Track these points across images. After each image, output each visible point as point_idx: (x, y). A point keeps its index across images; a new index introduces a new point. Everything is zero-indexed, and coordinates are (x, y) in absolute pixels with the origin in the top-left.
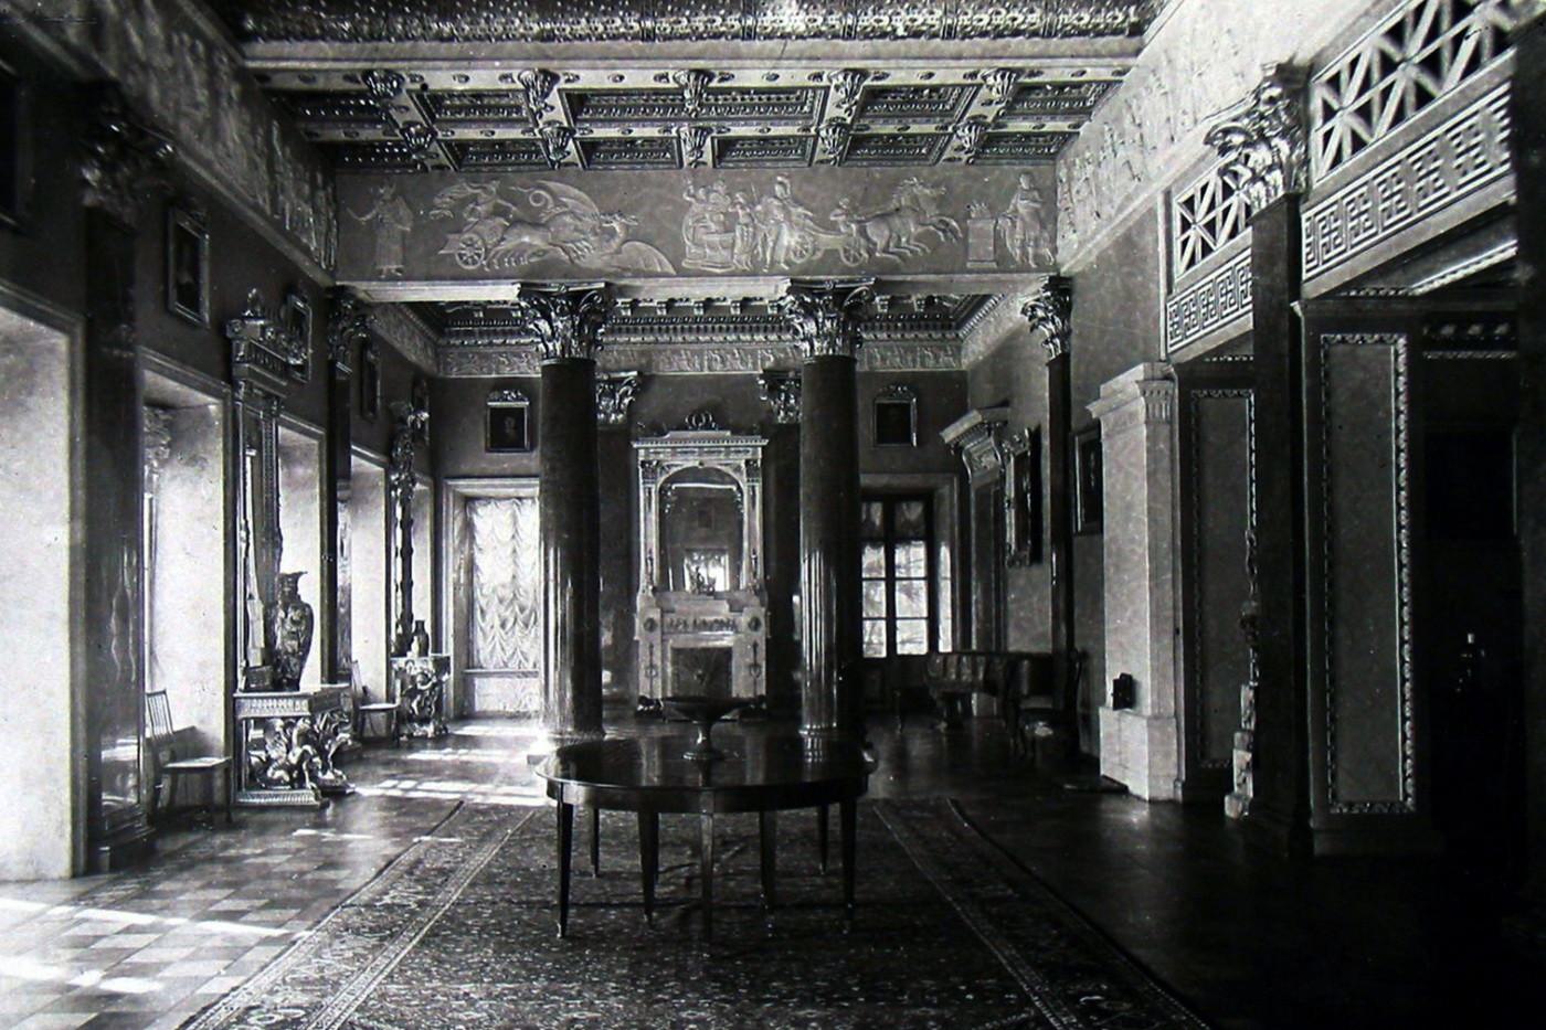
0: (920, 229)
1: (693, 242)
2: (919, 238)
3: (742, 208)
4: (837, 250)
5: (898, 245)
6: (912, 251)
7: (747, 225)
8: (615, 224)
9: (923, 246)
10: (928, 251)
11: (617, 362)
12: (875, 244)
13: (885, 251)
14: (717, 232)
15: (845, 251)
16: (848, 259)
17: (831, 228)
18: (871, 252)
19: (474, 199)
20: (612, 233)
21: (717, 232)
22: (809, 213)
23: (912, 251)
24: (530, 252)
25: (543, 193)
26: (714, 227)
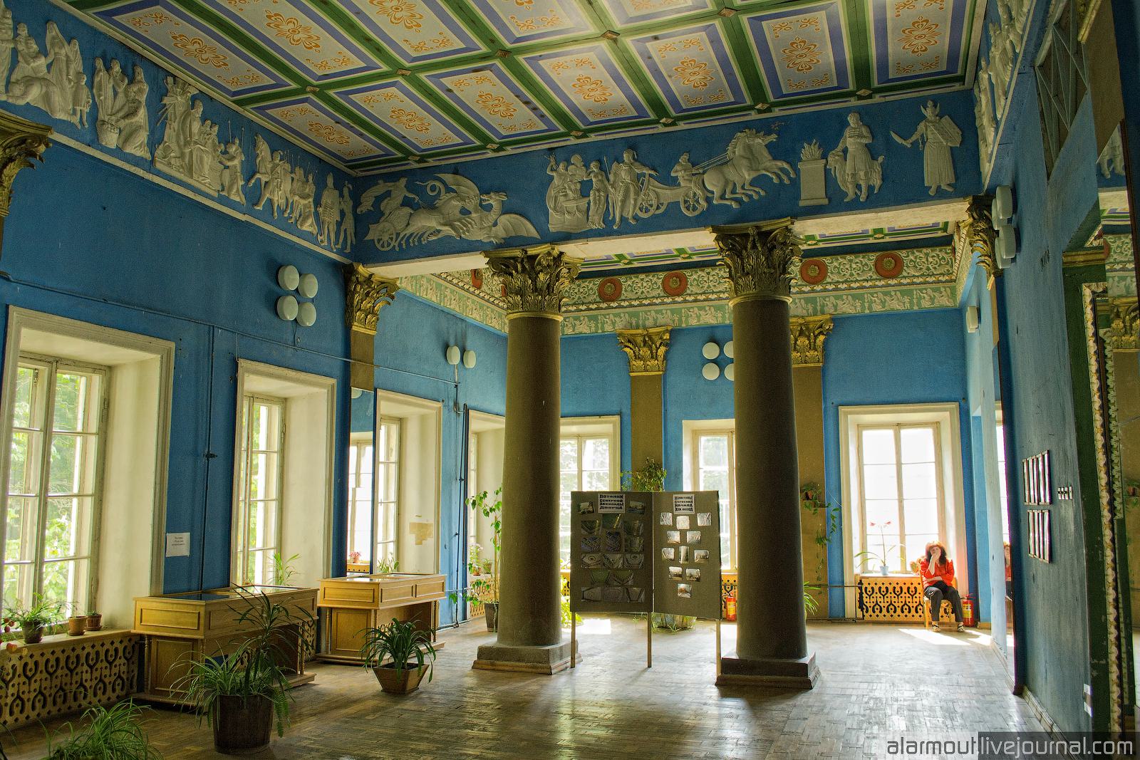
0: (754, 175)
1: (555, 209)
2: (753, 183)
5: (733, 192)
6: (747, 195)
7: (598, 191)
8: (491, 202)
9: (757, 189)
10: (762, 193)
11: (655, 320)
12: (713, 193)
13: (722, 197)
15: (686, 202)
16: (688, 208)
17: (674, 183)
18: (708, 200)
19: (388, 194)
20: (489, 208)
22: (652, 172)
23: (747, 195)
24: (428, 233)
25: (438, 184)
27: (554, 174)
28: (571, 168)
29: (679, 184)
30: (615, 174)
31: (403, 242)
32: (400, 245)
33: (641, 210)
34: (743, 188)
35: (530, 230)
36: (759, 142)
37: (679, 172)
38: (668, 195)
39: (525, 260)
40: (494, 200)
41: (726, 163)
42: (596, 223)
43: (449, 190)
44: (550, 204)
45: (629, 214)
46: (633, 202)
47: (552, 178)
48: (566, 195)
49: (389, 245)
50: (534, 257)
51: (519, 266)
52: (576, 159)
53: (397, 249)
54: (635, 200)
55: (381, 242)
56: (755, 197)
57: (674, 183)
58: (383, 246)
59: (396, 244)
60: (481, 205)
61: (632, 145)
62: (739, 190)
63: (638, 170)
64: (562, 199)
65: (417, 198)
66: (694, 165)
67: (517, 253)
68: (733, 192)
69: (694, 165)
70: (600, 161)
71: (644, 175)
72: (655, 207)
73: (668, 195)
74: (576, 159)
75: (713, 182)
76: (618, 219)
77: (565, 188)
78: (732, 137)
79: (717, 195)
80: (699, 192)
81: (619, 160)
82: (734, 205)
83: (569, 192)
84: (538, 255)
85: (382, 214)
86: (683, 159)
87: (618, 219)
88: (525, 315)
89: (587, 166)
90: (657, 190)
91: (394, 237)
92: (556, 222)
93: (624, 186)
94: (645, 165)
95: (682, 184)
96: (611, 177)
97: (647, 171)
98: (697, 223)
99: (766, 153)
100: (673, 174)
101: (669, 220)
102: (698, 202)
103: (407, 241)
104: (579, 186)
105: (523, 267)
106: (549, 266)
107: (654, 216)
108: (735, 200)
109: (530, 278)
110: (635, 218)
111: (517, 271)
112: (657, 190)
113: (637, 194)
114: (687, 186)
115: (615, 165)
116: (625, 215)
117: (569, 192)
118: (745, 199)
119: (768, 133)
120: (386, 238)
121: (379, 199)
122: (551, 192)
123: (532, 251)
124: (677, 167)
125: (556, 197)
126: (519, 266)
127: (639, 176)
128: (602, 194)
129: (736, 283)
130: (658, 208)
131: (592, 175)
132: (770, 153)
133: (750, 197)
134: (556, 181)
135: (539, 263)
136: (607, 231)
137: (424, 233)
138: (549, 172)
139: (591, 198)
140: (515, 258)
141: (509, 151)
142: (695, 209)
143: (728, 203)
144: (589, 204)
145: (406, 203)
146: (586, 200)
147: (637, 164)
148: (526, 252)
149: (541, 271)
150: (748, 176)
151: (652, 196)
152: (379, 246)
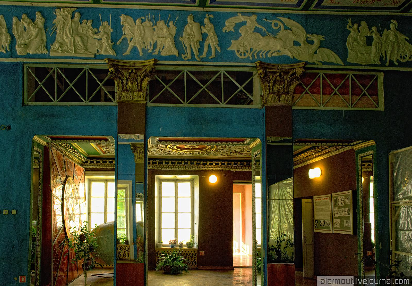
1: (351, 50)
3: (376, 35)
20: (312, 43)
31: (255, 54)
32: (253, 56)
40: (316, 39)
43: (286, 28)
48: (358, 43)
49: (245, 55)
53: (251, 59)
55: (240, 53)
58: (241, 55)
59: (250, 56)
60: (307, 40)
64: (355, 44)
65: (264, 30)
85: (240, 35)
89: (370, 28)
91: (249, 51)
103: (258, 55)
104: (365, 39)
120: (242, 50)
121: (238, 26)
122: (349, 40)
137: (270, 51)
138: (348, 28)
145: (256, 30)
152: (238, 55)
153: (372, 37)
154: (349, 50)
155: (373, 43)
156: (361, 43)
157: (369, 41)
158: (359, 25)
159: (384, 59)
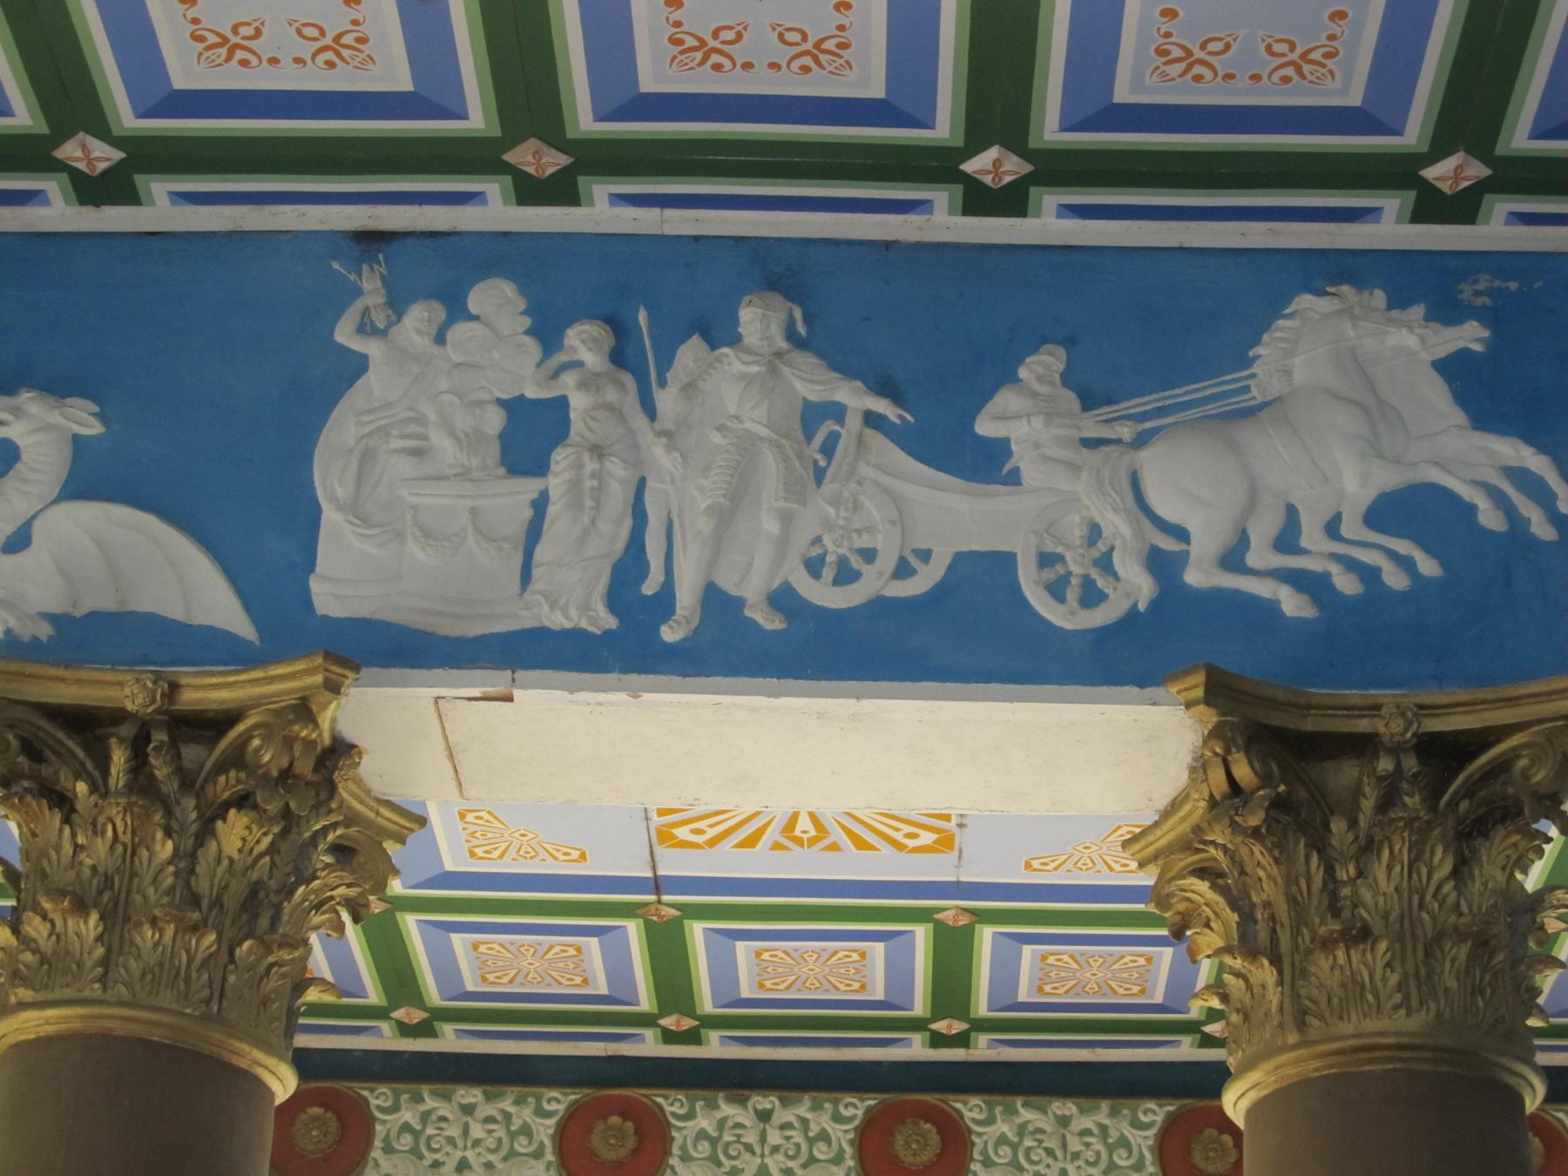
0: (1389, 478)
1: (356, 510)
4: (1006, 561)
5: (1287, 541)
6: (1352, 565)
7: (598, 451)
9: (1403, 547)
10: (1428, 567)
12: (1181, 534)
13: (1233, 559)
14: (463, 475)
15: (1046, 560)
16: (1056, 591)
17: (989, 464)
18: (1162, 565)
21: (463, 475)
22: (882, 406)
23: (1352, 565)
26: (445, 448)
27: (372, 348)
28: (460, 331)
29: (1014, 478)
30: (689, 388)
33: (814, 567)
34: (1332, 529)
35: (205, 595)
36: (1411, 344)
37: (1008, 417)
38: (953, 518)
39: (160, 736)
41: (1250, 413)
42: (573, 598)
44: (330, 480)
45: (750, 591)
46: (771, 526)
47: (358, 366)
50: (211, 725)
51: (119, 758)
52: (497, 301)
54: (786, 519)
56: (1395, 579)
57: (989, 464)
61: (778, 269)
62: (1312, 536)
63: (811, 381)
64: (403, 466)
66: (1089, 401)
67: (130, 692)
68: (1287, 541)
69: (1089, 401)
70: (620, 327)
71: (837, 412)
72: (886, 562)
73: (953, 518)
74: (497, 301)
75: (1196, 491)
76: (687, 597)
77: (421, 420)
78: (1275, 307)
79: (1205, 544)
80: (1117, 525)
81: (717, 331)
82: (1292, 604)
83: (442, 443)
84: (229, 718)
86: (1042, 368)
87: (687, 597)
88: (117, 1020)
89: (547, 332)
90: (898, 485)
92: (349, 574)
93: (736, 452)
94: (844, 367)
95: (1029, 475)
96: (666, 400)
97: (855, 398)
98: (1115, 659)
99: (1438, 394)
100: (985, 427)
101: (960, 634)
102: (1105, 564)
104: (495, 420)
105: (139, 763)
106: (287, 774)
107: (881, 607)
108: (1297, 580)
109: (168, 833)
110: (783, 599)
111: (99, 787)
112: (898, 485)
113: (794, 490)
114: (1061, 488)
115: (691, 352)
116: (727, 582)
117: (442, 443)
118: (1347, 584)
119: (1447, 311)
122: (343, 430)
123: (206, 690)
124: (1006, 399)
125: (367, 456)
126: (119, 758)
127: (814, 415)
128: (616, 468)
129: (1293, 975)
130: (903, 570)
131: (569, 379)
132: (1460, 399)
133: (1369, 575)
134: (377, 383)
135: (237, 759)
136: (633, 640)
138: (345, 334)
139: (557, 481)
140: (118, 716)
141: (161, 207)
142: (1091, 597)
143: (1262, 588)
144: (540, 505)
146: (529, 488)
147: (807, 360)
148: (174, 687)
149: (243, 801)
150: (1357, 483)
151: (873, 509)
153: (562, 403)
154: (331, 516)
155: (561, 458)
156: (445, 448)
157: (530, 436)
158: (457, 310)
159: (649, 588)
